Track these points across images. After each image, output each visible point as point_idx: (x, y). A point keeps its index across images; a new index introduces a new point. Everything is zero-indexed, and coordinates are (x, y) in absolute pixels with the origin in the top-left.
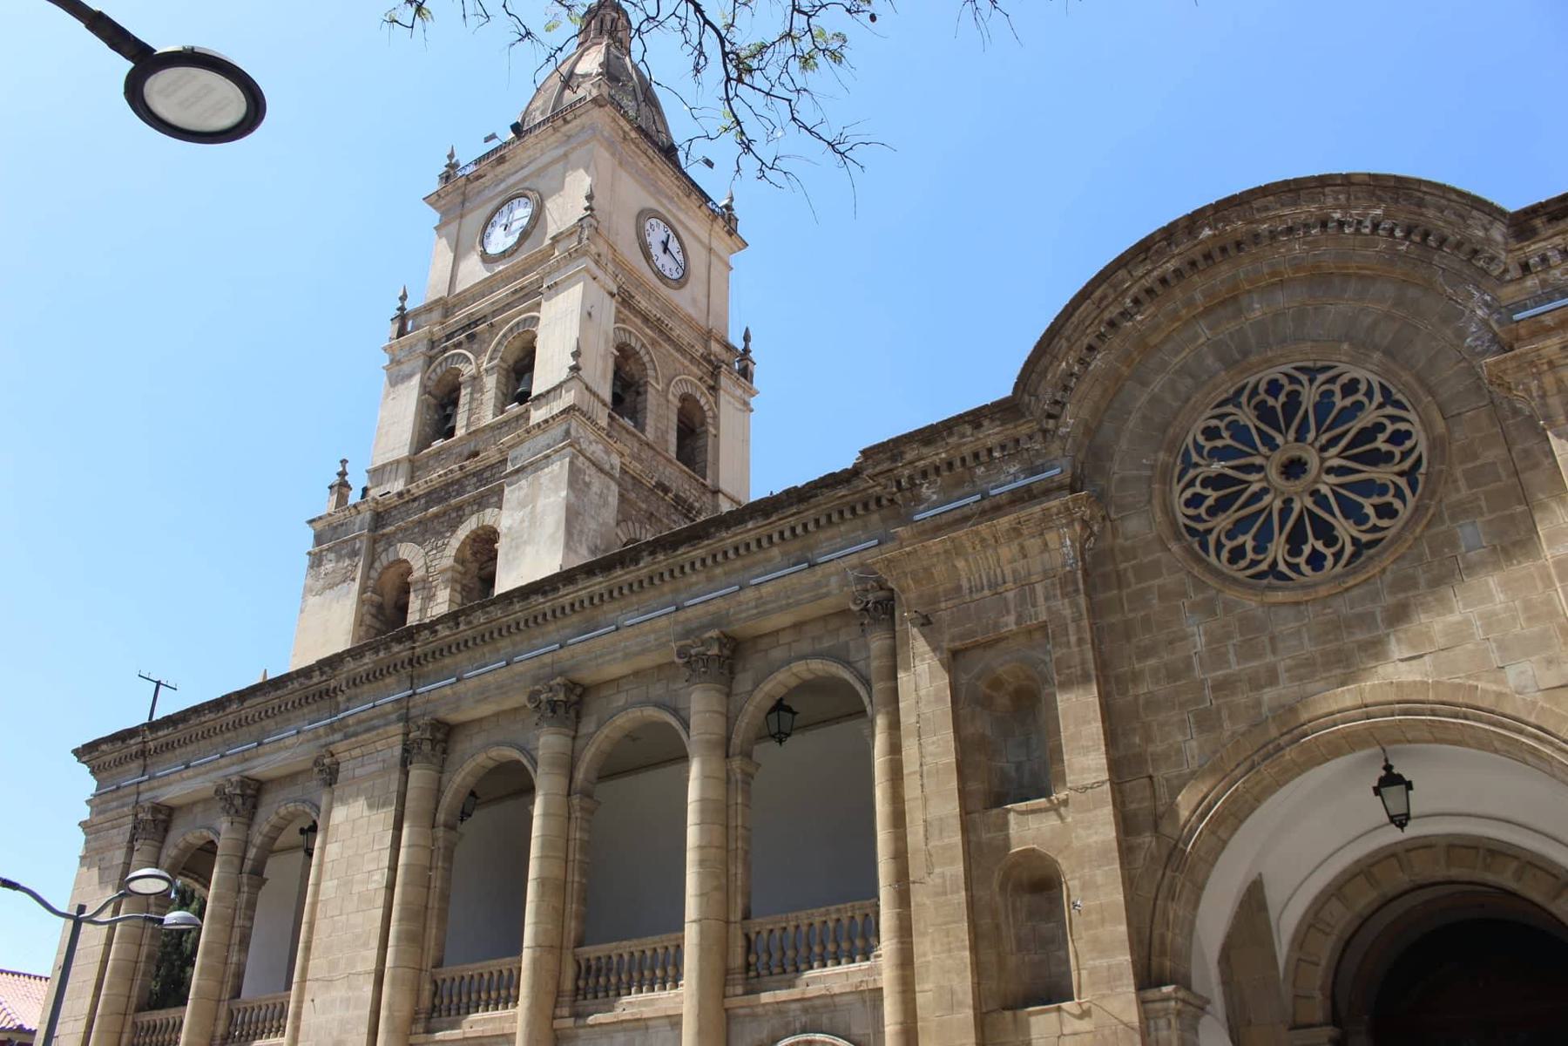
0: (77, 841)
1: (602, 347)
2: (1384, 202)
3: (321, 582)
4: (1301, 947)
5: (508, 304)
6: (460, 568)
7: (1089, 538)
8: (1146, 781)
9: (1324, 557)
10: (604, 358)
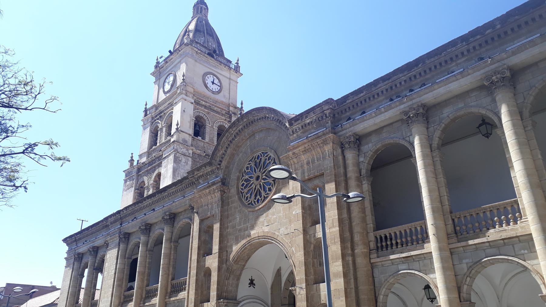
0: (64, 262)
1: (189, 119)
5: (168, 107)
6: (155, 183)
7: (224, 194)
8: (226, 252)
10: (190, 122)
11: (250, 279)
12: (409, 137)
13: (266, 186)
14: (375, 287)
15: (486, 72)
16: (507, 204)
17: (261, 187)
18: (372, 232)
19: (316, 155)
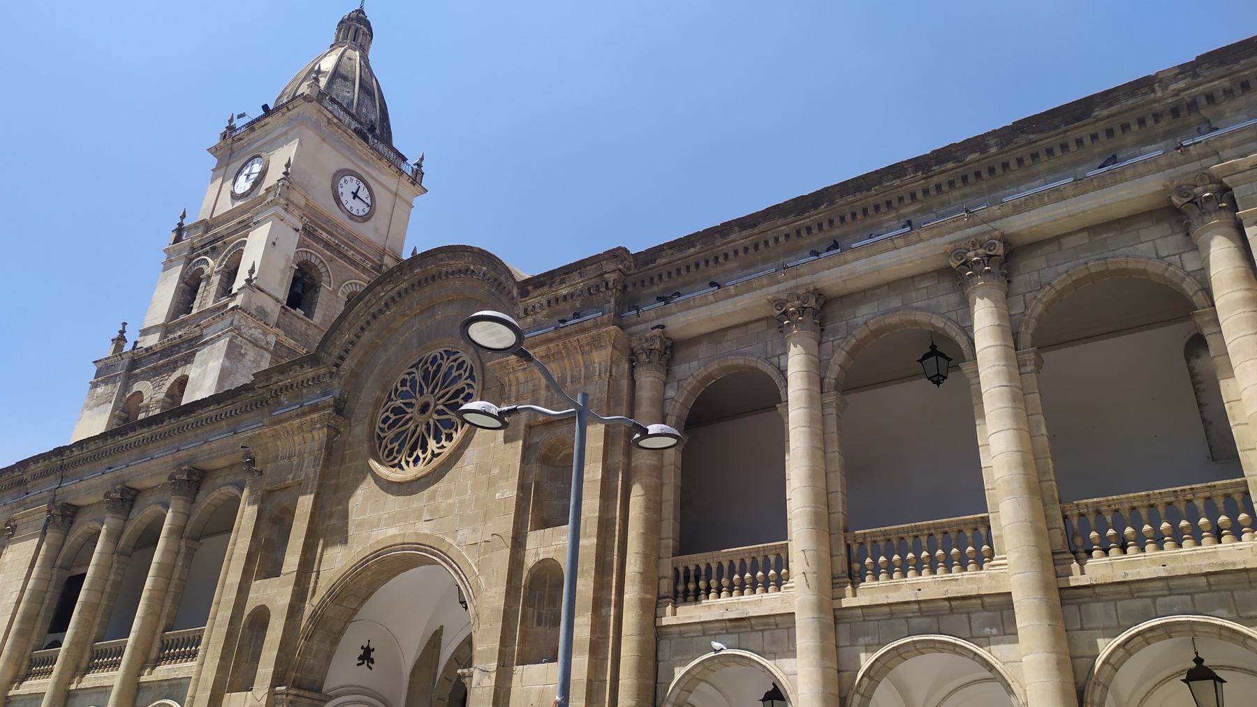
1: (282, 265)
6: (169, 400)
7: (336, 435)
10: (283, 272)
11: (365, 646)
12: (778, 356)
13: (442, 429)
14: (656, 683)
15: (958, 241)
16: (966, 523)
17: (428, 430)
18: (668, 558)
19: (571, 370)
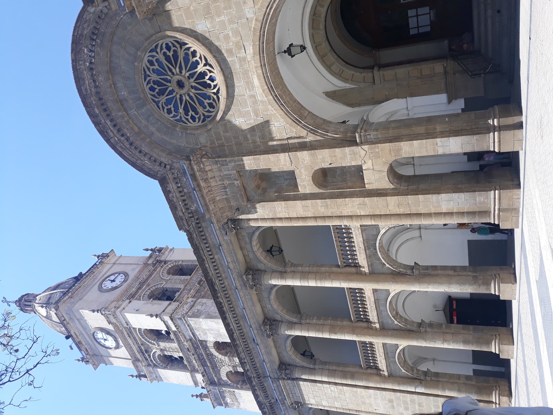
1: (149, 305)
2: (82, 48)
3: (235, 403)
4: (347, 80)
5: (134, 338)
6: (229, 354)
7: (207, 155)
9: (211, 76)
10: (153, 304)
